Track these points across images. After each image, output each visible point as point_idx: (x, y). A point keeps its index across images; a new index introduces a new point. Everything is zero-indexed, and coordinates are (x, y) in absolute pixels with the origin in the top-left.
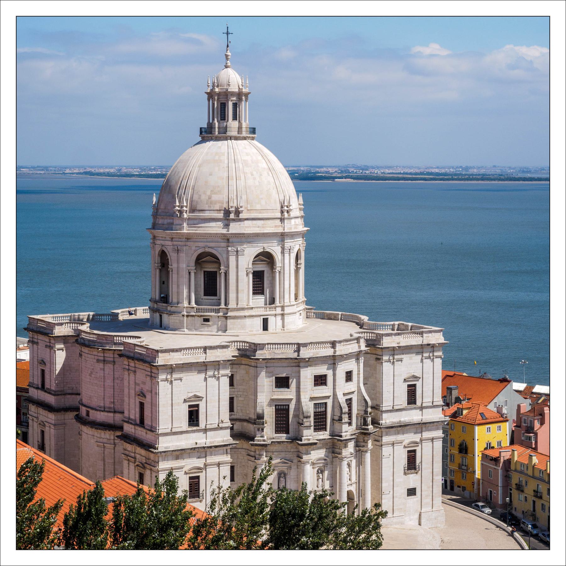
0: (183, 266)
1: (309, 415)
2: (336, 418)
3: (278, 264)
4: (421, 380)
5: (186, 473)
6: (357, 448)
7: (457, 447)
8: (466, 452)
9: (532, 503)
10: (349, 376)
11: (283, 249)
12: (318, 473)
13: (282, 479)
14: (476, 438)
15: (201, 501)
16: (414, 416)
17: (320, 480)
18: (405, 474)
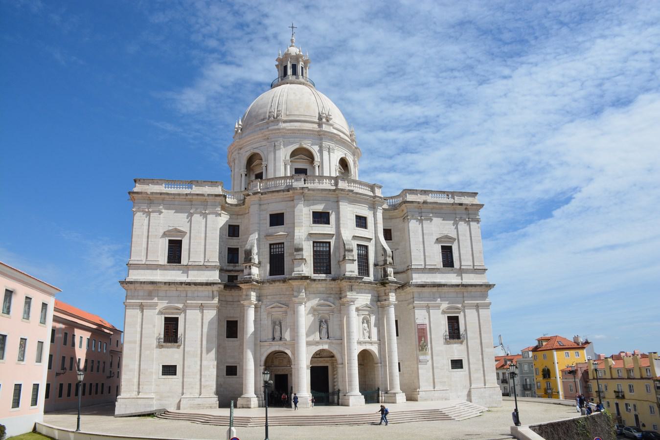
0: (237, 170)
1: (300, 247)
2: (341, 259)
3: (317, 158)
4: (457, 240)
5: (160, 313)
6: (379, 303)
7: (541, 373)
8: (549, 377)
9: (615, 405)
10: (361, 222)
11: (321, 147)
12: (321, 322)
13: (277, 327)
14: (556, 362)
15: (178, 347)
16: (451, 278)
17: (324, 331)
18: (447, 343)
